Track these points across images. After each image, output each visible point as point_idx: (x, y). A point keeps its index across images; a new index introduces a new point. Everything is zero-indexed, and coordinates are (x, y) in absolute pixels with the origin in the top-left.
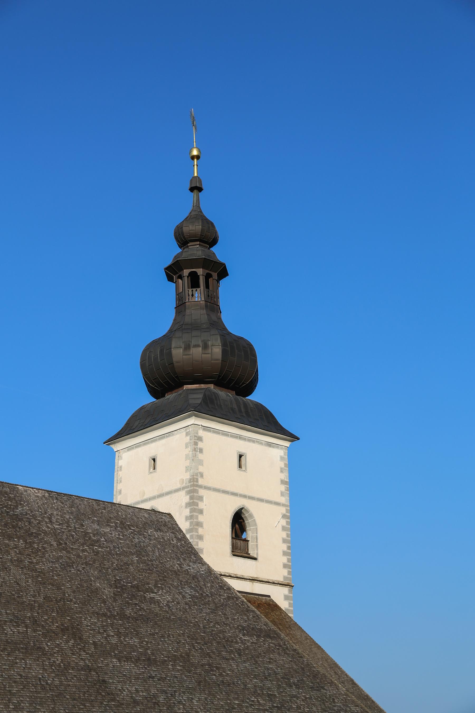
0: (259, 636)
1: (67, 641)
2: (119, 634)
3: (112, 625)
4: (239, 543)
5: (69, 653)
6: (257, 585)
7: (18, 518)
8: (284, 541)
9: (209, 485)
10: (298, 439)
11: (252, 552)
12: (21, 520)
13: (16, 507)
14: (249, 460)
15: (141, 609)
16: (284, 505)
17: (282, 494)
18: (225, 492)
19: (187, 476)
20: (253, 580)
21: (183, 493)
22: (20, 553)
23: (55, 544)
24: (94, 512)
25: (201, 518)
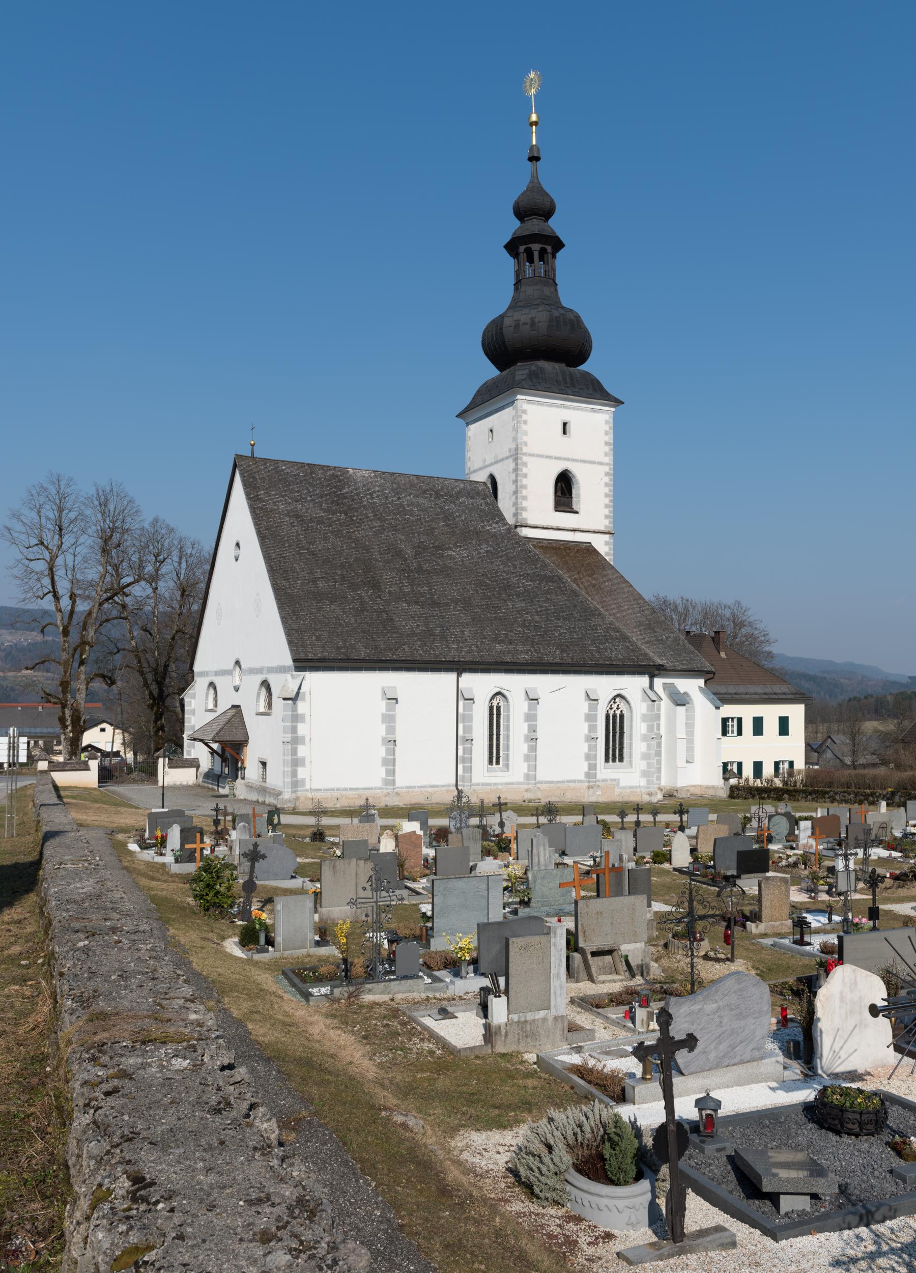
0: (541, 581)
1: (367, 591)
2: (412, 585)
3: (408, 578)
4: (563, 500)
5: (367, 599)
6: (577, 534)
7: (344, 496)
8: (607, 495)
9: (533, 452)
10: (623, 403)
11: (575, 507)
12: (346, 497)
13: (344, 488)
14: (571, 428)
15: (437, 564)
16: (607, 464)
17: (606, 454)
18: (548, 457)
19: (513, 446)
20: (574, 530)
21: (511, 460)
22: (341, 525)
23: (371, 515)
24: (412, 486)
25: (525, 481)
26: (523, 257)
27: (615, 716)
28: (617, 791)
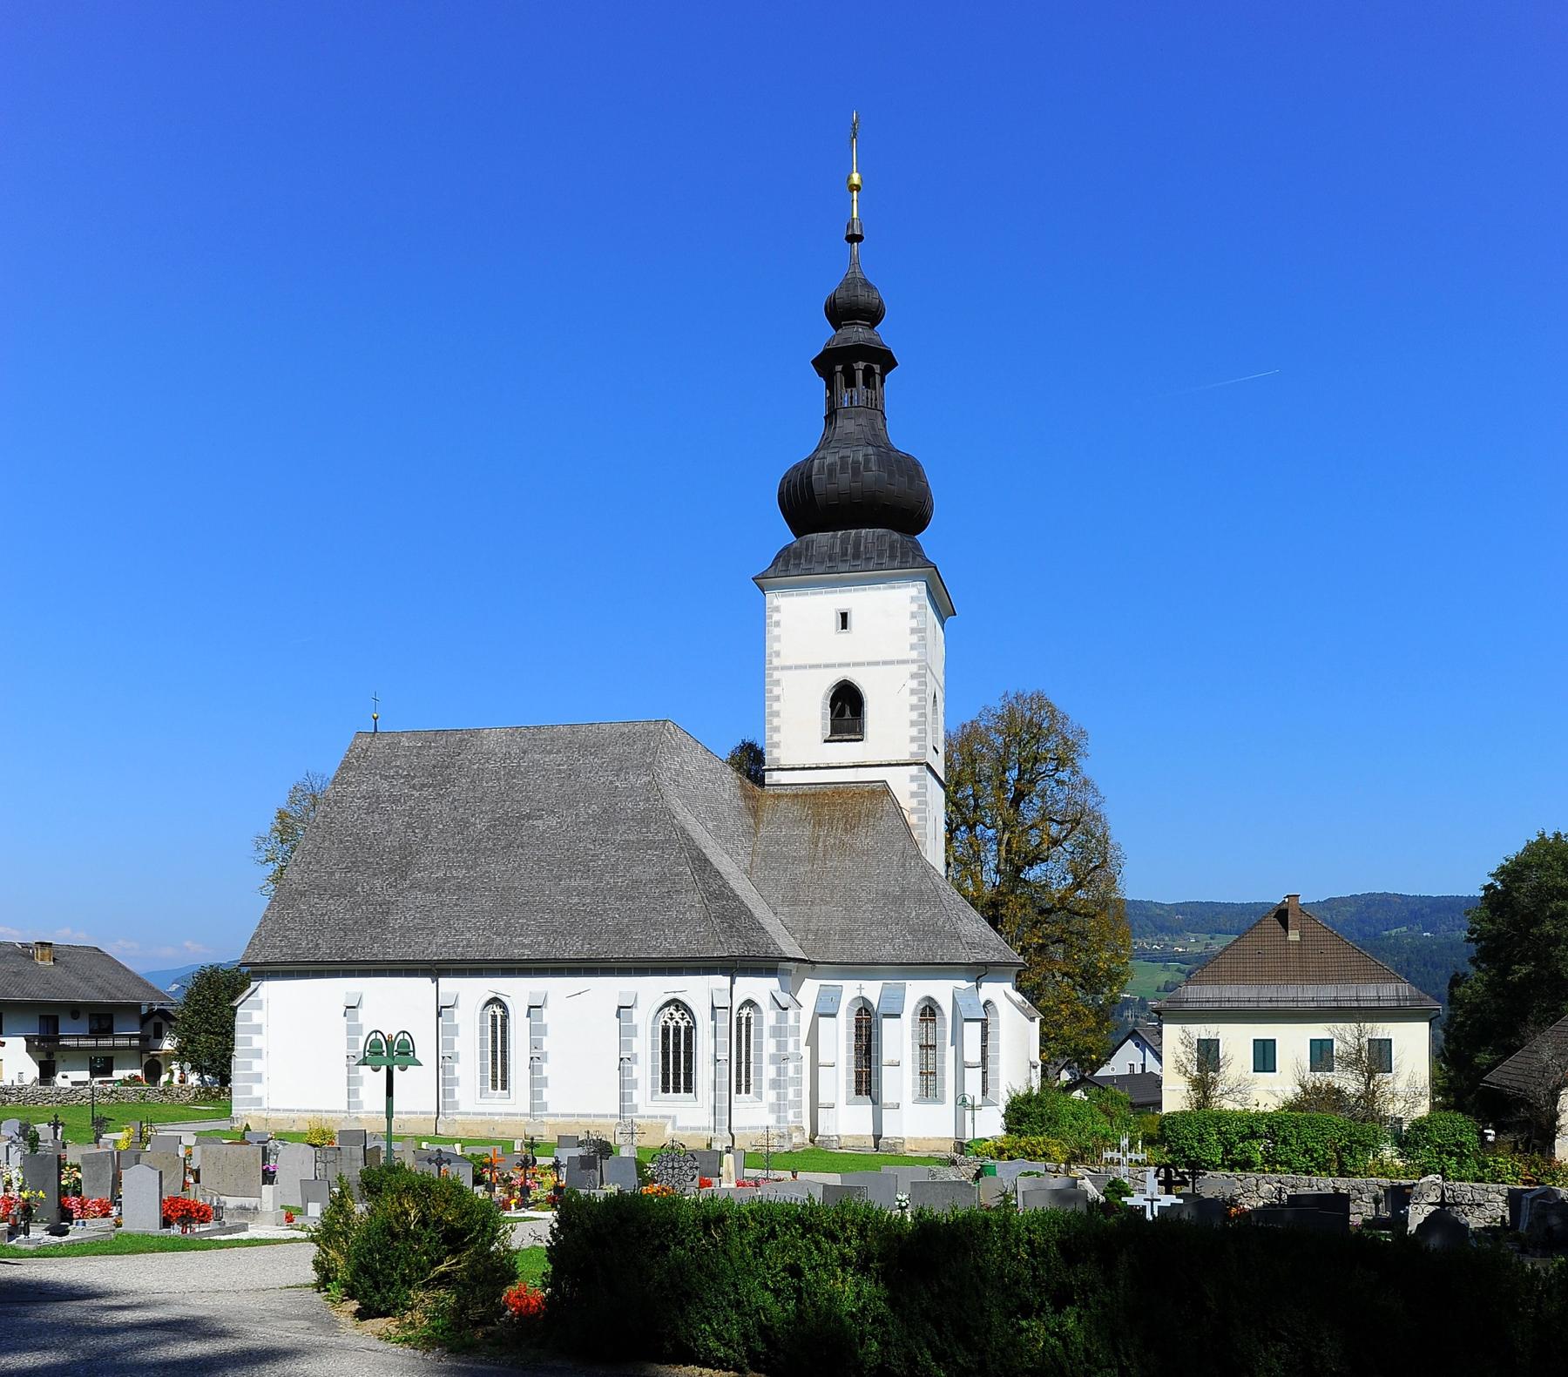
14: (853, 620)
26: (840, 379)
27: (677, 1030)
28: (669, 1131)
